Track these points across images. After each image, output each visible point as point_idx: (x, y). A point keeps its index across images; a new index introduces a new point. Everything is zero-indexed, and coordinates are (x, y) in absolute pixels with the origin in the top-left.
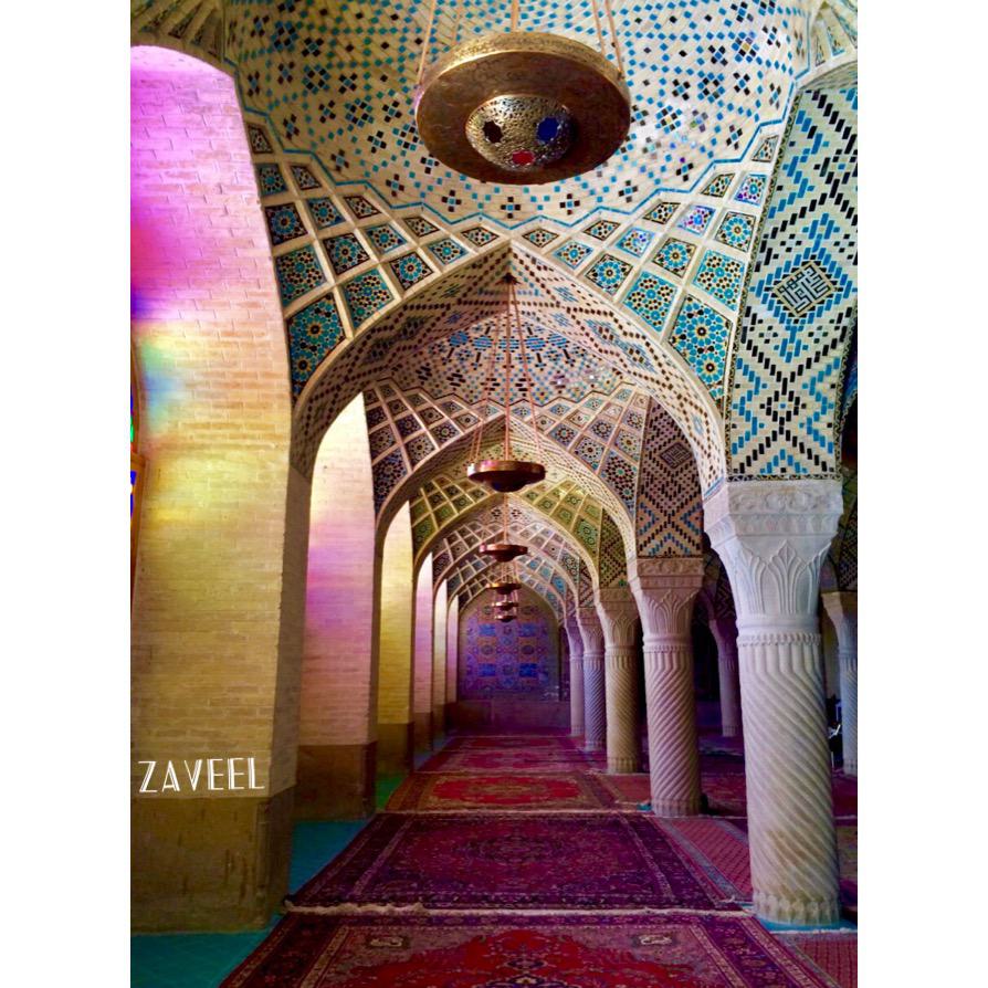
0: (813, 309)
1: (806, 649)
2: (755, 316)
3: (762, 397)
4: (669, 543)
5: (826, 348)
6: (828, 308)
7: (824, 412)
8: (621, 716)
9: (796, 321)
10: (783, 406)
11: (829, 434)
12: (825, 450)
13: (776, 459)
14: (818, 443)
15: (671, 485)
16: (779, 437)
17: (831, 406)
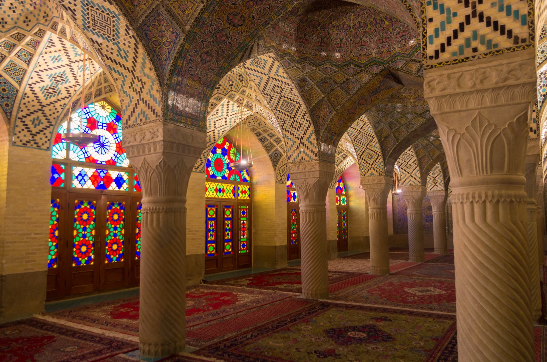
0: (114, 31)
1: (155, 215)
2: (97, 42)
10: (137, 85)
12: (157, 105)
15: (295, 123)
17: (154, 81)
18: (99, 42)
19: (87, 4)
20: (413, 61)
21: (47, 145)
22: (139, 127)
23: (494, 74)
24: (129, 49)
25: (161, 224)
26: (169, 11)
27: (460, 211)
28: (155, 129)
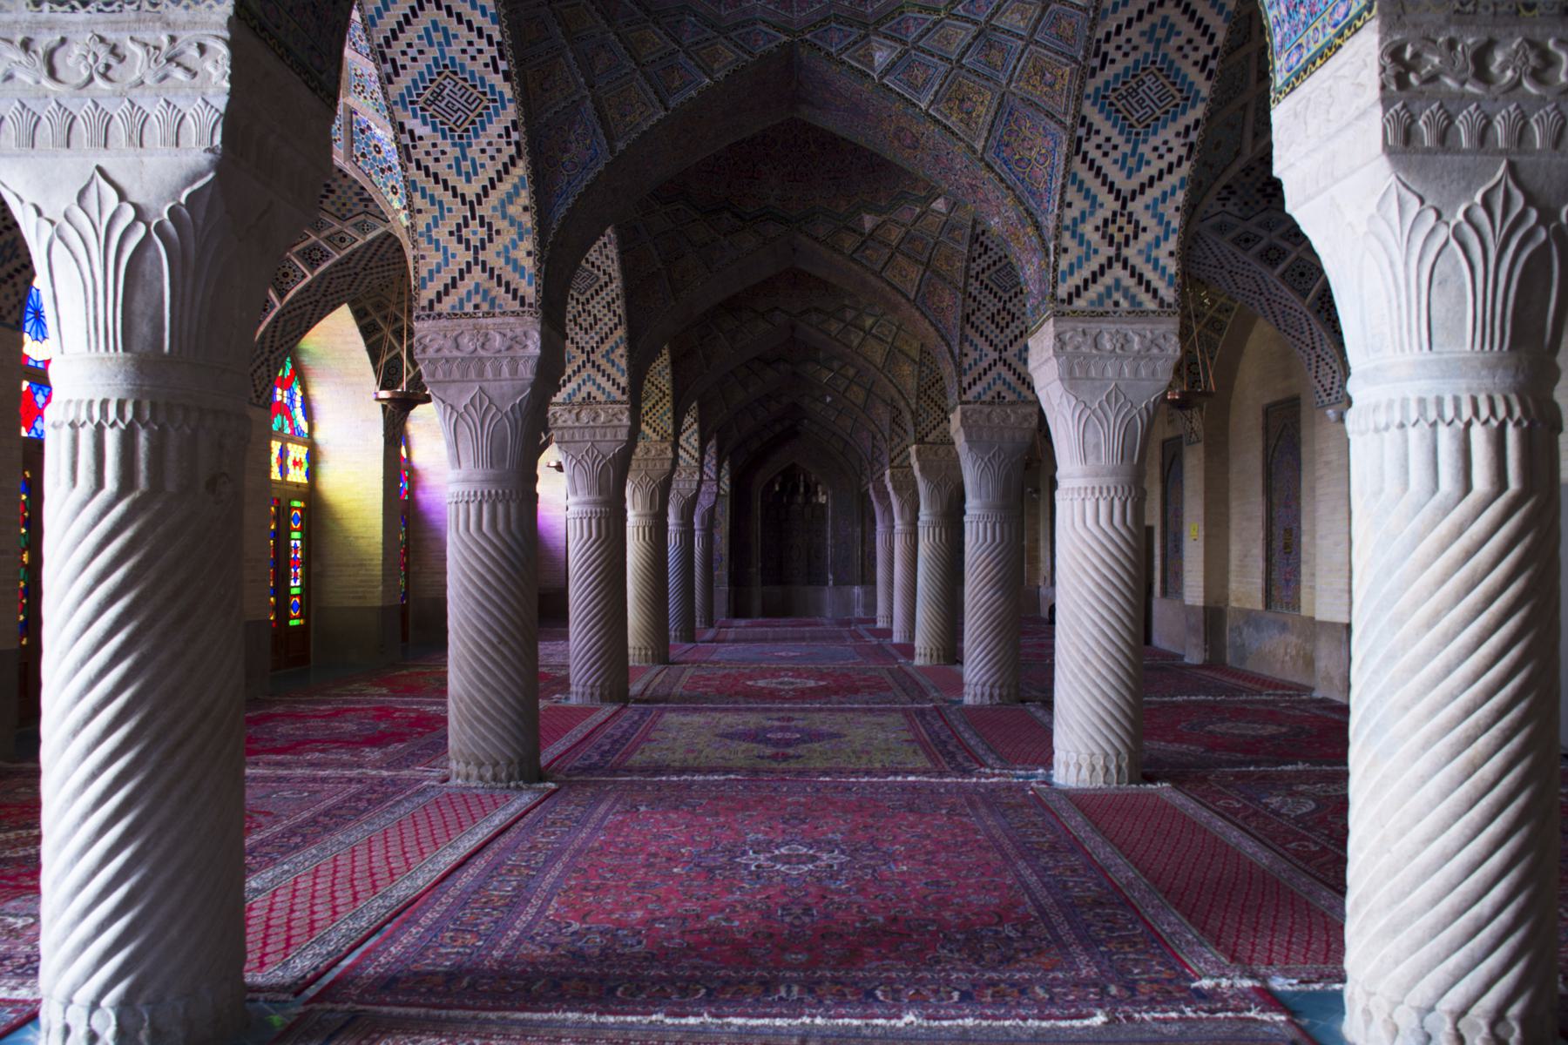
0: (473, 122)
1: (500, 508)
2: (411, 132)
3: (451, 223)
4: (589, 387)
5: (505, 165)
6: (491, 122)
7: (521, 239)
8: (640, 599)
9: (461, 137)
10: (475, 233)
11: (528, 263)
12: (524, 283)
13: (469, 292)
14: (517, 276)
15: (584, 315)
16: (474, 268)
18: (417, 133)
19: (446, 66)
20: (848, 229)
21: (16, 315)
22: (472, 321)
23: (1136, 339)
24: (488, 162)
25: (513, 526)
26: (598, 109)
27: (1068, 512)
28: (519, 331)
